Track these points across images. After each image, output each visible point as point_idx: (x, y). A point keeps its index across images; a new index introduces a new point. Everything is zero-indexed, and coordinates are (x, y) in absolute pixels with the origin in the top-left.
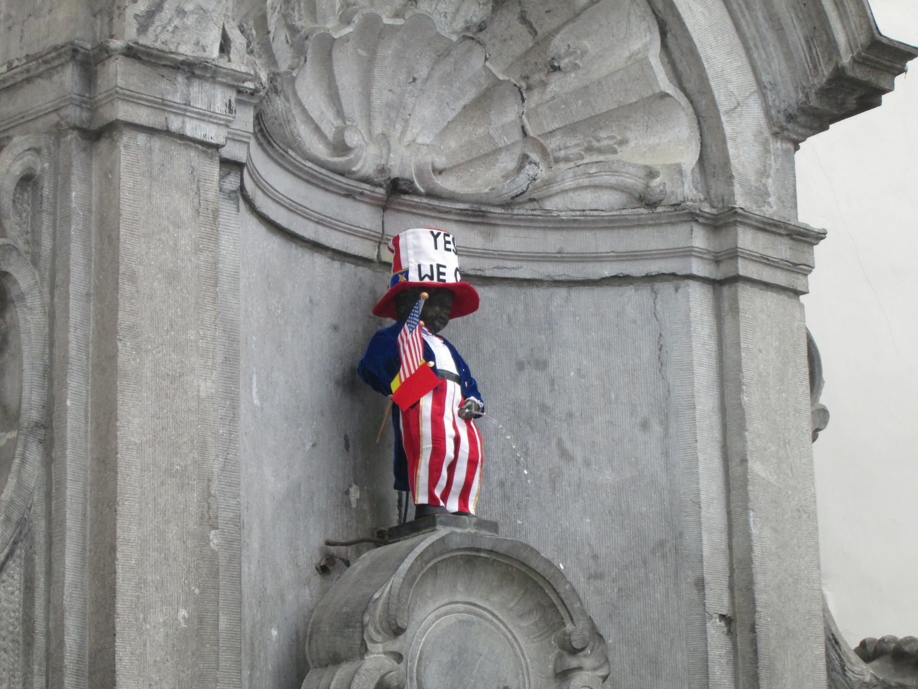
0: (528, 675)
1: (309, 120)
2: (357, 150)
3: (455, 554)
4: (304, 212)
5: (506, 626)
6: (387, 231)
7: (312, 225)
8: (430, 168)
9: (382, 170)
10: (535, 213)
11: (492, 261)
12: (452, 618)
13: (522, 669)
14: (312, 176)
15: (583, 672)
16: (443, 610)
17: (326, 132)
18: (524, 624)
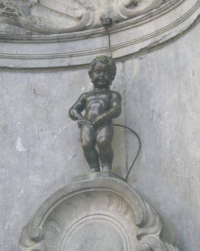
0: (129, 243)
1: (62, 14)
2: (84, 16)
3: (75, 194)
4: (60, 56)
5: (117, 221)
6: (111, 45)
7: (68, 59)
8: (124, 7)
9: (101, 19)
10: (167, 4)
11: (161, 35)
12: (84, 224)
13: (126, 241)
14: (58, 39)
15: (148, 235)
16: (80, 222)
17: (71, 15)
18: (127, 217)
